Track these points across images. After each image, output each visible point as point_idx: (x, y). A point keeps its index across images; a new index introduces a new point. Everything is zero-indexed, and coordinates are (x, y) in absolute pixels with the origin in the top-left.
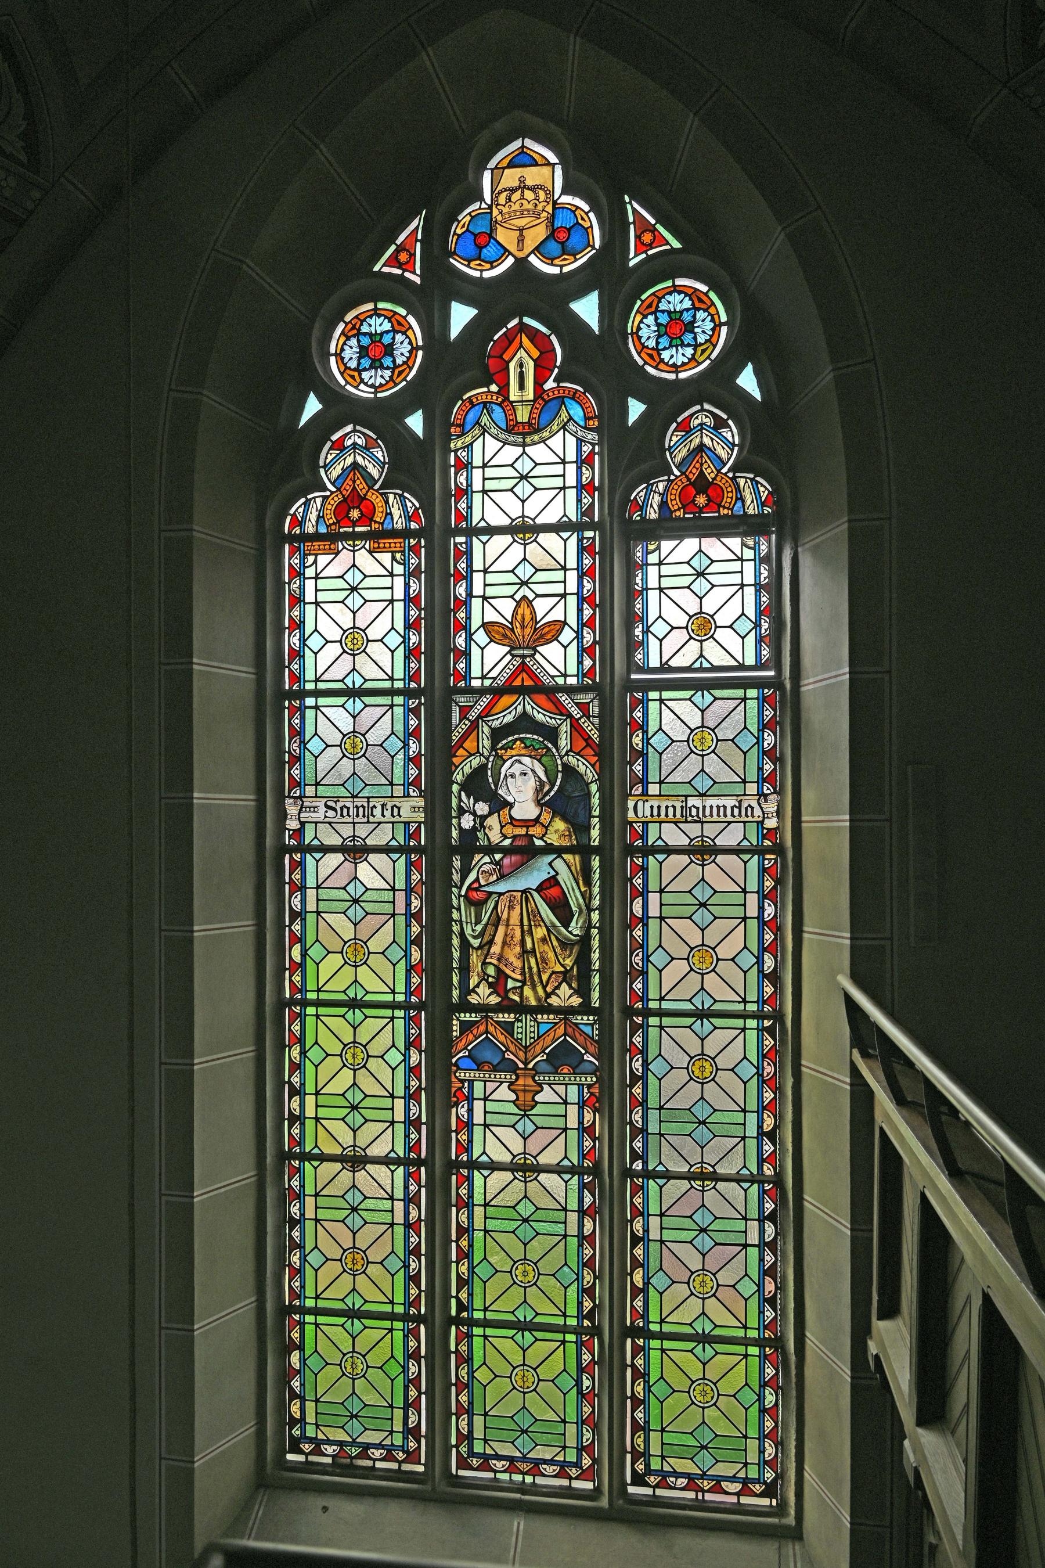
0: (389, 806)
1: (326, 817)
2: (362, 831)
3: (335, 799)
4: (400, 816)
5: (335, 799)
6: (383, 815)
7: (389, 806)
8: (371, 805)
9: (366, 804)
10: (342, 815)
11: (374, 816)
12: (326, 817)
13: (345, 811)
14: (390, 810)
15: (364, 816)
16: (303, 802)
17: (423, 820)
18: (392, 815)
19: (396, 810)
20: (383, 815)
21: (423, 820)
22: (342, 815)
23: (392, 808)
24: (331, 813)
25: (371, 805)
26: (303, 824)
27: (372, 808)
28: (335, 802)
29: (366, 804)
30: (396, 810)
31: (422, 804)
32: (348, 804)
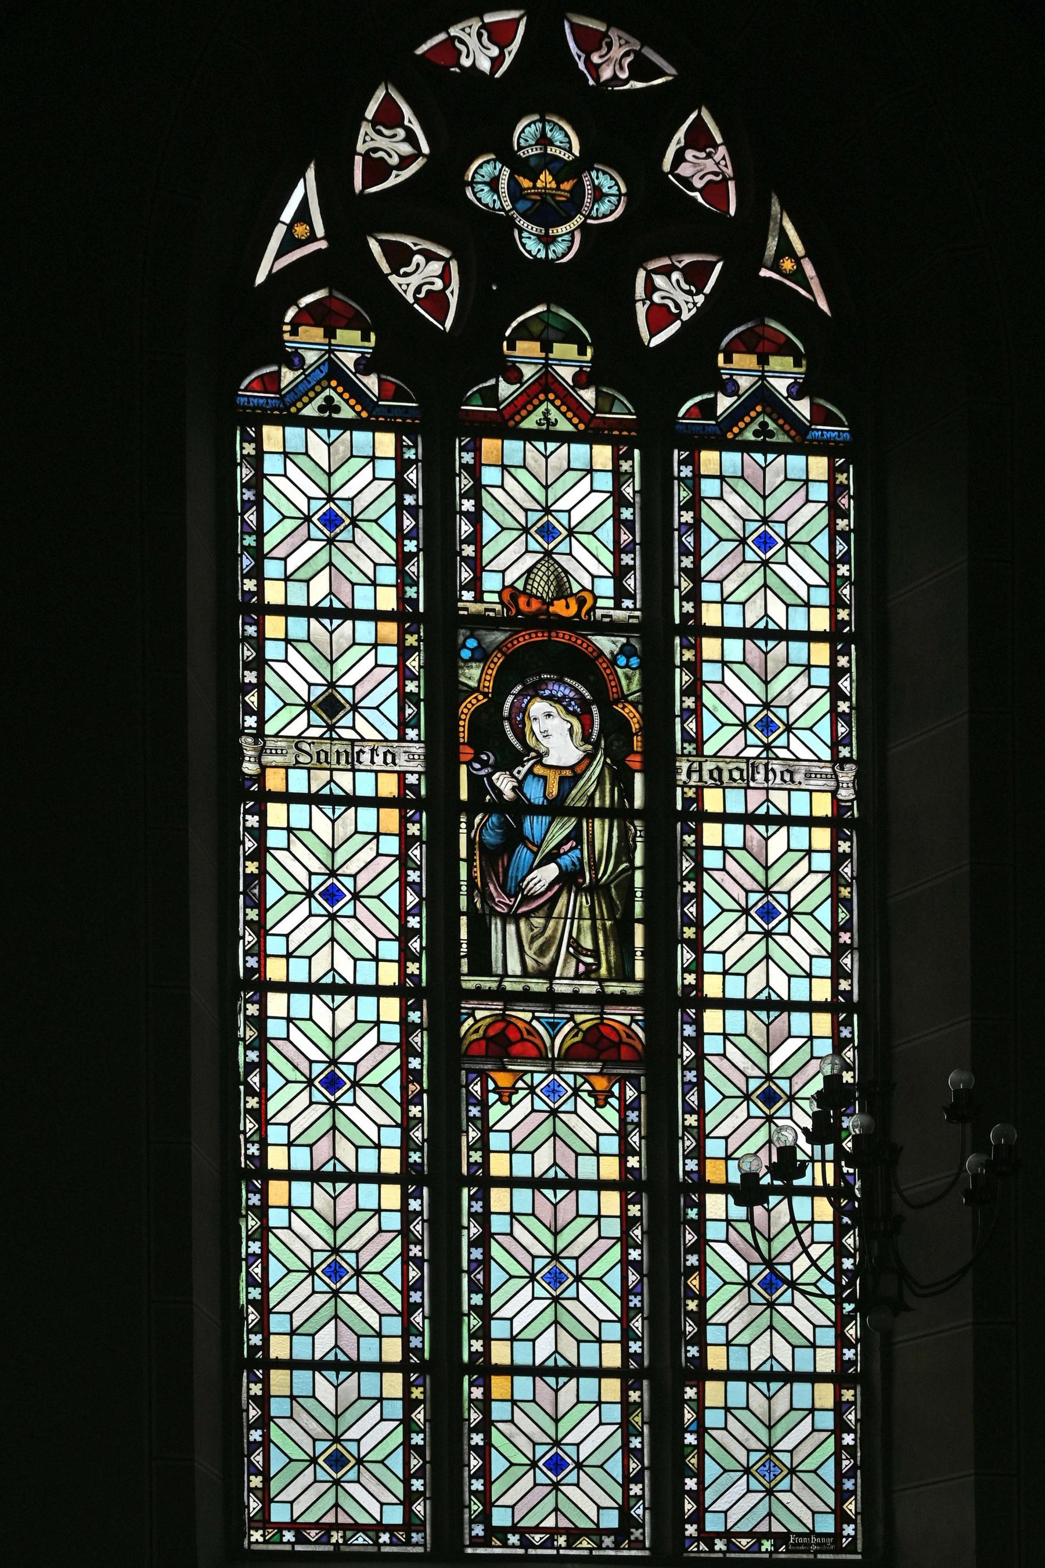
0: (381, 751)
1: (297, 762)
3: (309, 741)
4: (395, 765)
5: (309, 741)
6: (372, 762)
7: (381, 751)
8: (356, 749)
9: (349, 750)
10: (318, 760)
11: (361, 763)
12: (297, 762)
13: (323, 756)
14: (381, 756)
15: (347, 762)
16: (265, 742)
20: (372, 762)
22: (318, 760)
23: (385, 754)
24: (304, 759)
25: (356, 749)
26: (263, 768)
27: (358, 753)
28: (309, 744)
29: (349, 750)
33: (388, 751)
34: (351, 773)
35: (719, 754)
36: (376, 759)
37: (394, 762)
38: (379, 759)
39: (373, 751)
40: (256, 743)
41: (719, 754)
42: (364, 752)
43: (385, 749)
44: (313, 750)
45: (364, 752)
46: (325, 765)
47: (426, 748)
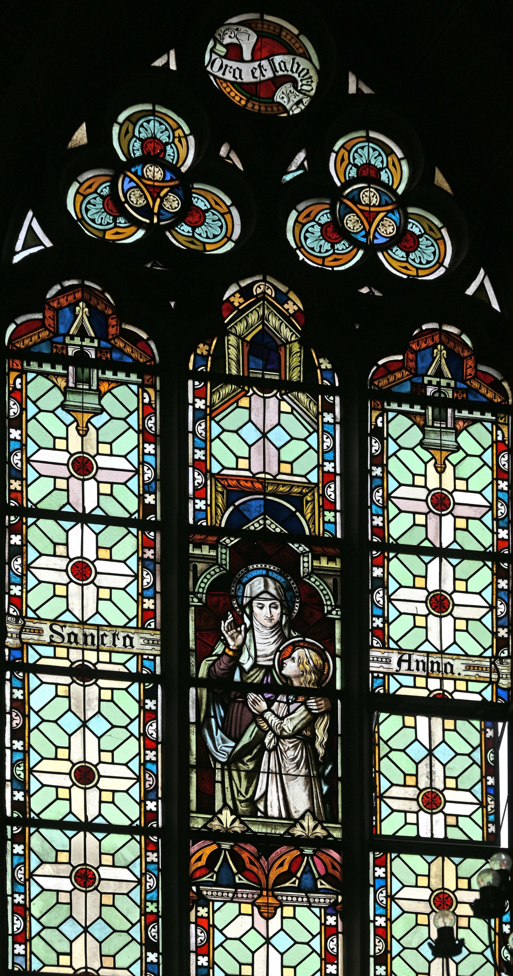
0: (121, 635)
2: (91, 656)
6: (114, 644)
7: (121, 635)
12: (52, 641)
16: (25, 622)
17: (159, 653)
18: (125, 645)
19: (128, 640)
21: (159, 653)
23: (124, 638)
30: (128, 640)
31: (158, 637)
32: (76, 631)
33: (128, 636)
34: (96, 653)
35: (419, 649)
36: (117, 642)
37: (132, 645)
38: (119, 643)
39: (114, 635)
40: (17, 622)
41: (419, 649)
42: (106, 636)
43: (126, 634)
44: (66, 631)
45: (106, 636)
46: (74, 645)
47: (162, 635)
